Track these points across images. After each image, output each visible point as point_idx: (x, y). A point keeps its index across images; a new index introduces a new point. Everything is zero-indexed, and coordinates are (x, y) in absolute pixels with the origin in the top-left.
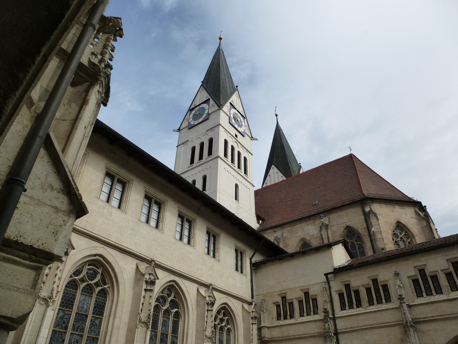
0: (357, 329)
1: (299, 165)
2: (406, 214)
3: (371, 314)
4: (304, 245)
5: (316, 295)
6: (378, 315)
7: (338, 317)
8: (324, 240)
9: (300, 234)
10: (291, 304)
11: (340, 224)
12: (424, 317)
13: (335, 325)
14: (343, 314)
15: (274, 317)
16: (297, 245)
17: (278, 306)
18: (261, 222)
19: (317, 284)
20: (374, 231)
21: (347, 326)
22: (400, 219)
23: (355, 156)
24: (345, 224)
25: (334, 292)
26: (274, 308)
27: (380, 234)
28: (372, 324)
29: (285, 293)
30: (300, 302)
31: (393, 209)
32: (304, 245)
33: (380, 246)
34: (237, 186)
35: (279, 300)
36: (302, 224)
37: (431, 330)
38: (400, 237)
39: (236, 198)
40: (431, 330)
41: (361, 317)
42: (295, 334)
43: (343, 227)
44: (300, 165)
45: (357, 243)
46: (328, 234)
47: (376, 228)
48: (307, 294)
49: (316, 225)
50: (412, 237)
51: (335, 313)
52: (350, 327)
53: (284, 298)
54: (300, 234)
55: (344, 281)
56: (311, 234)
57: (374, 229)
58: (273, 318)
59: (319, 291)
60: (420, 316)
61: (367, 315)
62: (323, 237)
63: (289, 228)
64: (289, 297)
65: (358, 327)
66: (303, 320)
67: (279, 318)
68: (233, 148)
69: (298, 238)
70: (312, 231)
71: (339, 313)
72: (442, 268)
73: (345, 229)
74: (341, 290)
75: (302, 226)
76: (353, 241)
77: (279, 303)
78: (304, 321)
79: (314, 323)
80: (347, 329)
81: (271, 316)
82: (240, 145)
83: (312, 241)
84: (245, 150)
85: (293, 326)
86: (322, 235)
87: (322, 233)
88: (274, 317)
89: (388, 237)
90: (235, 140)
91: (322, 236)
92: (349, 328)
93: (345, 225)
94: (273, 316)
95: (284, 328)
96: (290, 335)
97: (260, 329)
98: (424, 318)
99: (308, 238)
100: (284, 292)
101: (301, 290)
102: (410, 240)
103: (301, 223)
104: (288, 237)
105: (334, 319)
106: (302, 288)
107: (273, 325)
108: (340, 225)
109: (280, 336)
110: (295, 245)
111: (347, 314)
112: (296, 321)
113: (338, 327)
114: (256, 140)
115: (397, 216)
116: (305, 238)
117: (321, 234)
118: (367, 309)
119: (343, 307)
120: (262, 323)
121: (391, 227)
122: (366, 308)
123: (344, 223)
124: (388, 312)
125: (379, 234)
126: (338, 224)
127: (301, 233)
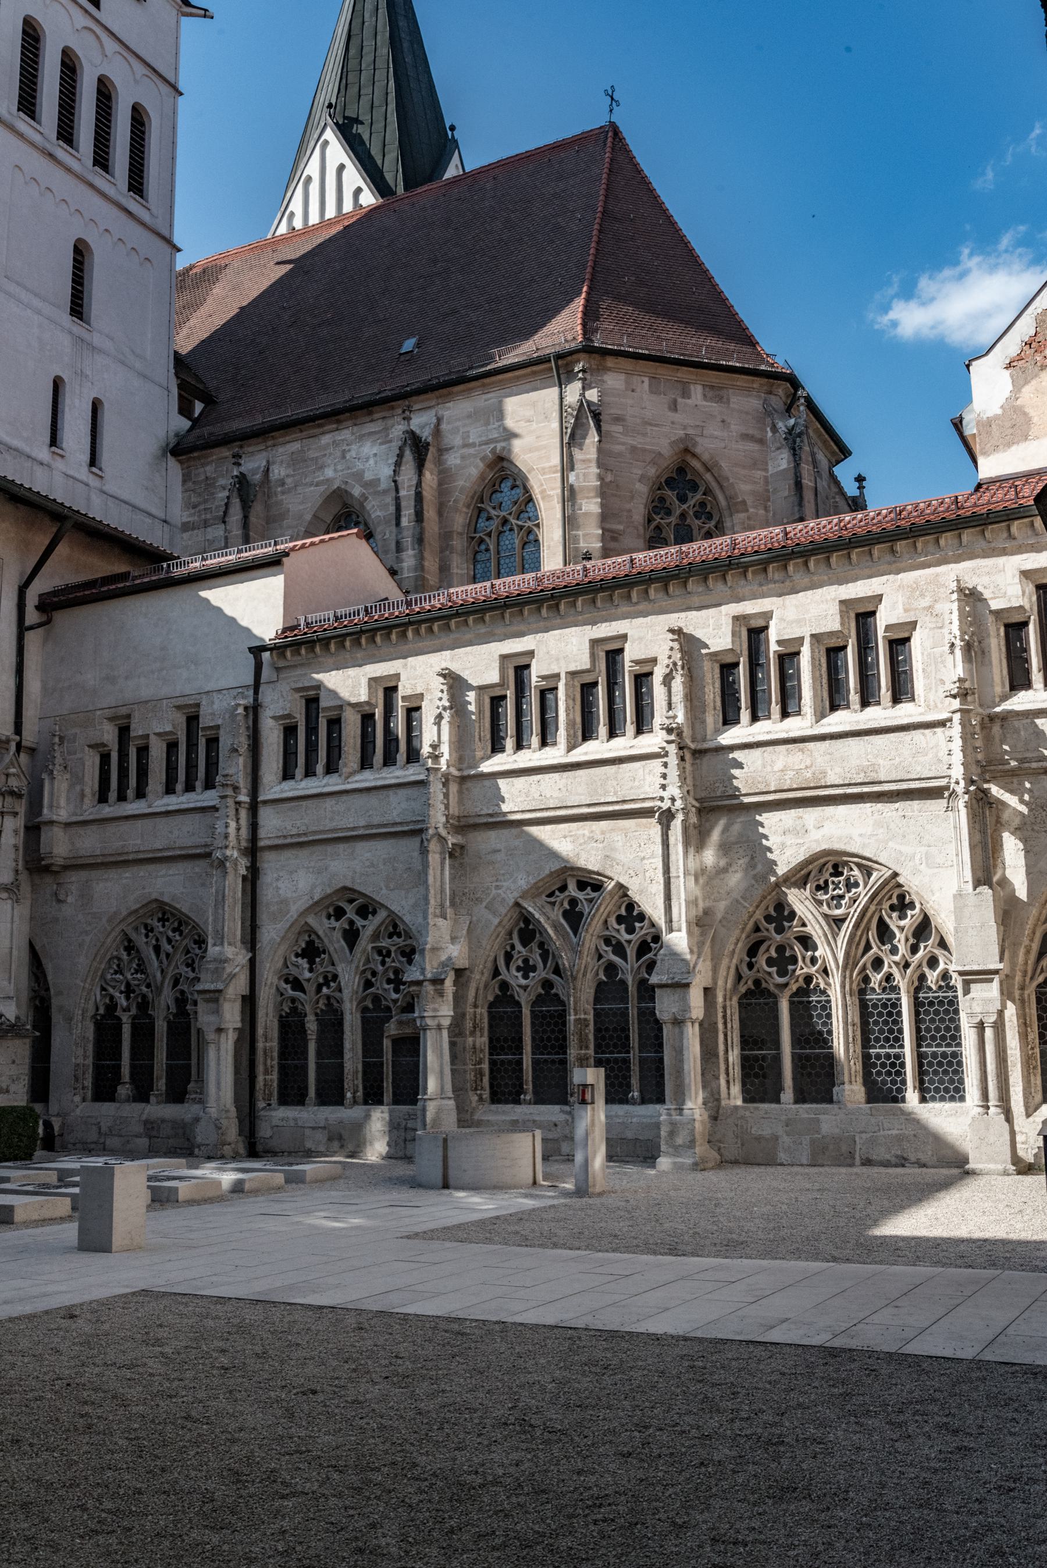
0: (311, 838)
1: (450, 133)
2: (723, 421)
3: (356, 796)
4: (343, 518)
5: (218, 727)
6: (373, 800)
7: (265, 802)
8: (403, 504)
9: (329, 473)
10: (143, 751)
11: (473, 445)
12: (490, 812)
13: (254, 827)
14: (282, 791)
15: (88, 791)
16: (315, 516)
17: (105, 758)
18: (198, 407)
20: (576, 485)
22: (698, 439)
23: (622, 140)
24: (492, 446)
25: (271, 720)
26: (92, 762)
27: (592, 497)
28: (352, 825)
29: (129, 716)
30: (172, 747)
31: (680, 400)
32: (343, 518)
33: (582, 545)
34: (81, 253)
35: (109, 735)
36: (346, 431)
37: (500, 851)
38: (678, 512)
39: (78, 308)
40: (500, 851)
41: (329, 803)
42: (142, 849)
43: (483, 459)
44: (453, 135)
45: (520, 523)
46: (419, 484)
47: (584, 475)
49: (390, 441)
50: (726, 513)
51: (261, 790)
52: (294, 832)
53: (124, 731)
54: (329, 473)
55: (301, 685)
56: (368, 476)
57: (577, 476)
58: (83, 795)
59: (227, 716)
61: (344, 798)
62: (403, 493)
63: (296, 446)
64: (137, 730)
65: (315, 833)
66: (168, 805)
67: (103, 798)
68: (70, 66)
69: (322, 488)
70: (376, 463)
71: (273, 787)
72: (572, 668)
73: (491, 466)
74: (289, 716)
75: (343, 440)
76: (510, 514)
77: (105, 745)
78: (170, 808)
79: (197, 816)
80: (285, 837)
81: (78, 788)
82: (110, 45)
83: (368, 506)
84: (140, 69)
85: (139, 823)
86: (400, 486)
88: (88, 791)
89: (630, 511)
90: (82, 21)
91: (397, 490)
92: (292, 836)
93: (487, 450)
94: (83, 790)
95: (111, 828)
96: (126, 850)
97: (33, 830)
98: (491, 815)
99: (357, 491)
100: (124, 711)
101: (178, 708)
102: (713, 523)
103: (337, 430)
104: (289, 481)
105: (254, 808)
106: (181, 702)
107: (81, 818)
108: (472, 451)
109: (98, 852)
110: (308, 517)
111: (290, 794)
112: (150, 806)
113: (262, 833)
114: (205, 16)
116: (346, 491)
117: (395, 481)
118: (350, 780)
119: (287, 775)
120: (45, 811)
121: (652, 471)
122: (348, 778)
123: (487, 443)
124: (402, 793)
125: (588, 498)
126: (466, 445)
127: (335, 470)
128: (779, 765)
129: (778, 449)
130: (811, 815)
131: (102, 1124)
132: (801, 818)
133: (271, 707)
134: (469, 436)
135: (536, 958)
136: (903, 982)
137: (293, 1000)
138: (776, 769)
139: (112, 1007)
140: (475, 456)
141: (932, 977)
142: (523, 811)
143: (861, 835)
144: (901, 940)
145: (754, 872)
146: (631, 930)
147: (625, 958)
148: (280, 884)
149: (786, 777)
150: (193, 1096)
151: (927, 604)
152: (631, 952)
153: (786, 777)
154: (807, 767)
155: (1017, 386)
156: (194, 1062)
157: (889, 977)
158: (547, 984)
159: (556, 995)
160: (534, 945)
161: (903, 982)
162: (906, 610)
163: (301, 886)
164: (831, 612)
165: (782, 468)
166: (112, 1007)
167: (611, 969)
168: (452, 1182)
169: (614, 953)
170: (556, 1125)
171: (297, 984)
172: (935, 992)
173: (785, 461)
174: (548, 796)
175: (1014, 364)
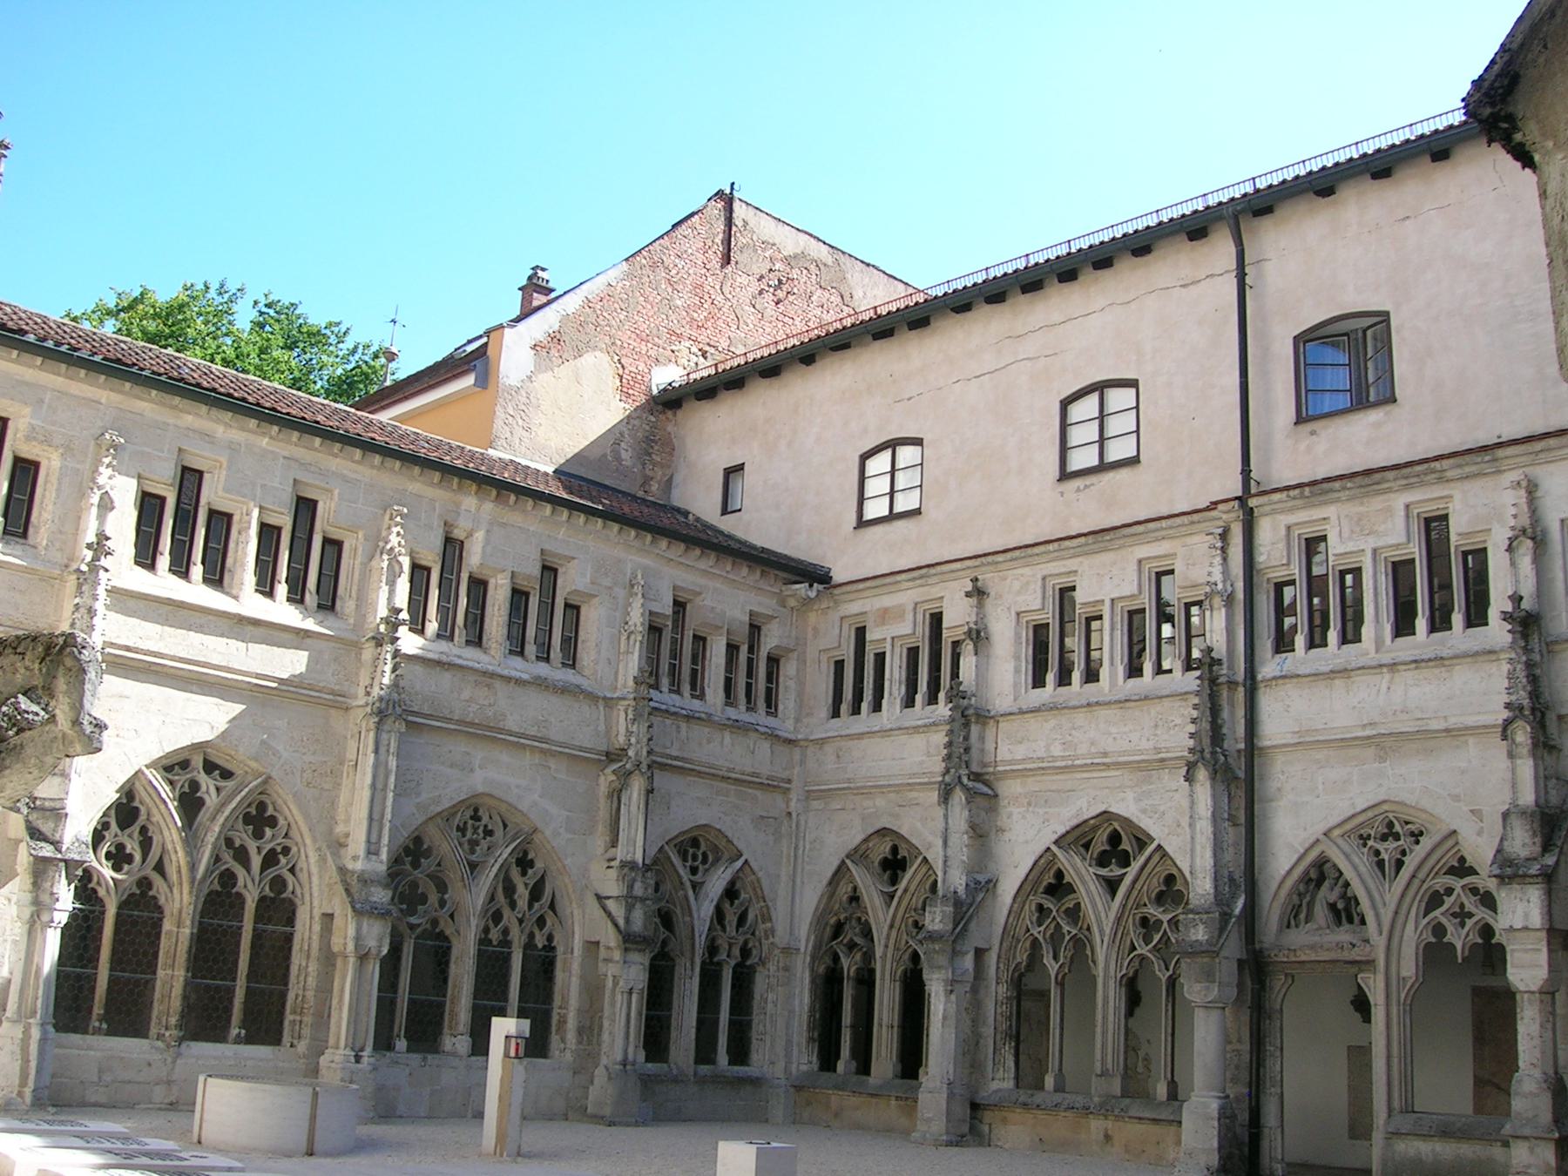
60: (118, 637)
98: (128, 649)
128: (466, 694)
130: (479, 753)
132: (468, 754)
135: (132, 847)
136: (517, 938)
138: (462, 697)
141: (540, 941)
143: (518, 787)
144: (522, 893)
145: (418, 800)
146: (258, 835)
147: (247, 868)
149: (470, 709)
151: (609, 584)
152: (256, 861)
153: (470, 709)
154: (490, 705)
155: (539, 368)
157: (506, 932)
158: (145, 883)
159: (154, 898)
160: (136, 828)
161: (517, 938)
162: (592, 583)
164: (533, 557)
167: (228, 878)
168: (318, 1147)
169: (235, 858)
170: (150, 1065)
172: (541, 950)
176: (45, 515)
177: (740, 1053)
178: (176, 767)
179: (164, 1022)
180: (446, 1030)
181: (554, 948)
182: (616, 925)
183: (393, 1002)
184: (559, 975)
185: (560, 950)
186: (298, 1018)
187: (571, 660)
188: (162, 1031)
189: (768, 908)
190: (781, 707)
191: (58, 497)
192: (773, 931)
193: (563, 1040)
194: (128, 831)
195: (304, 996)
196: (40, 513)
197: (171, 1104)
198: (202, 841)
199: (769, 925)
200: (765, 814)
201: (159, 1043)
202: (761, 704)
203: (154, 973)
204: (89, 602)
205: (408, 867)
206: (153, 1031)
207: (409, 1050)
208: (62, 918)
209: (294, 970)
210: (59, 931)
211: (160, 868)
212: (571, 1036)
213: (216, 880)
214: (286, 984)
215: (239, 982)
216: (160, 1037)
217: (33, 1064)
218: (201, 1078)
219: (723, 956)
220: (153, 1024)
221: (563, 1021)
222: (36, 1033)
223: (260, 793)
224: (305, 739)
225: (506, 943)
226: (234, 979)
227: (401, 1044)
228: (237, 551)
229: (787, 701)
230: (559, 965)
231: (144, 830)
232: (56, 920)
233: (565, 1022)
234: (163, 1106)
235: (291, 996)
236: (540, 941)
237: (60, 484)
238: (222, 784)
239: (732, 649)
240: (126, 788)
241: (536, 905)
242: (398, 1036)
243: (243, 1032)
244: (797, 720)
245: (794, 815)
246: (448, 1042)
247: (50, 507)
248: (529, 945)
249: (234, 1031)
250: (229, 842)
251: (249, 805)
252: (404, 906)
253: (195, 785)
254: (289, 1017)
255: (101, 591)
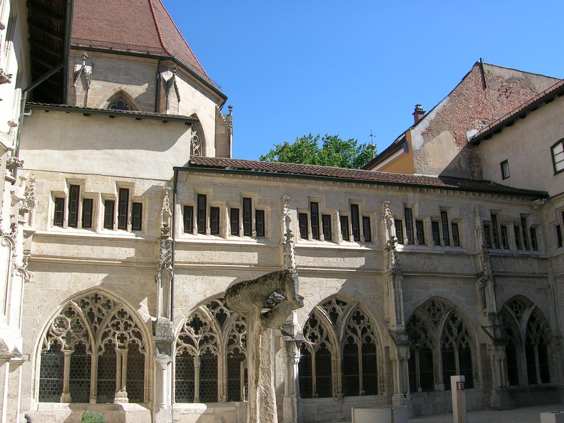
12: (305, 265)
19: (151, 180)
21: (191, 258)
43: (114, 90)
48: (124, 192)
52: (197, 261)
58: (46, 219)
59: (153, 193)
60: (300, 263)
80: (190, 263)
81: (44, 215)
87: (78, 86)
92: (194, 263)
98: (304, 267)
109: (59, 255)
115: (195, 105)
129: (222, 125)
131: (57, 415)
133: (182, 194)
134: (108, 77)
135: (317, 333)
137: (185, 348)
139: (56, 346)
140: (110, 87)
141: (464, 346)
142: (320, 267)
143: (447, 292)
145: (411, 303)
146: (359, 323)
148: (184, 287)
149: (425, 267)
150: (120, 399)
152: (359, 332)
153: (425, 267)
155: (425, 141)
156: (174, 380)
157: (451, 344)
158: (323, 345)
159: (327, 349)
160: (317, 327)
163: (198, 289)
165: (222, 133)
166: (56, 346)
167: (351, 339)
169: (352, 332)
171: (187, 340)
173: (224, 130)
174: (332, 262)
175: (424, 134)
176: (269, 228)
177: (546, 378)
178: (327, 304)
179: (337, 391)
180: (435, 382)
181: (469, 348)
182: (491, 336)
183: (415, 375)
184: (473, 358)
185: (472, 348)
186: (382, 384)
187: (457, 243)
188: (337, 395)
189: (547, 322)
190: (539, 247)
191: (272, 220)
192: (551, 330)
193: (478, 381)
194: (315, 328)
195: (383, 377)
196: (267, 227)
197: (343, 419)
198: (340, 328)
199: (549, 329)
200: (540, 287)
201: (336, 399)
202: (531, 246)
203: (331, 375)
204: (289, 254)
205: (412, 326)
206: (334, 395)
207: (423, 391)
208: (297, 360)
209: (378, 368)
210: (297, 364)
211: (327, 339)
212: (481, 379)
213: (347, 341)
214: (376, 373)
215: (360, 375)
216: (336, 396)
217: (296, 410)
218: (352, 409)
219: (533, 343)
220: (333, 392)
221: (477, 374)
222: (295, 400)
223: (357, 308)
224: (369, 287)
225: (451, 348)
226: (358, 374)
227: (420, 389)
228: (334, 227)
229: (541, 244)
230: (472, 353)
231: (320, 327)
232: (296, 361)
233: (478, 374)
234: (341, 420)
235: (379, 377)
236: (464, 346)
237: (272, 216)
238: (343, 307)
239: (516, 228)
240: (312, 313)
241: (461, 333)
242: (418, 386)
243: (364, 391)
244: (546, 251)
245: (551, 286)
246: (436, 387)
247: (270, 225)
248: (460, 348)
249: (361, 392)
250: (349, 327)
251: (354, 313)
252: (413, 340)
253: (334, 309)
254: (379, 384)
255: (292, 249)
